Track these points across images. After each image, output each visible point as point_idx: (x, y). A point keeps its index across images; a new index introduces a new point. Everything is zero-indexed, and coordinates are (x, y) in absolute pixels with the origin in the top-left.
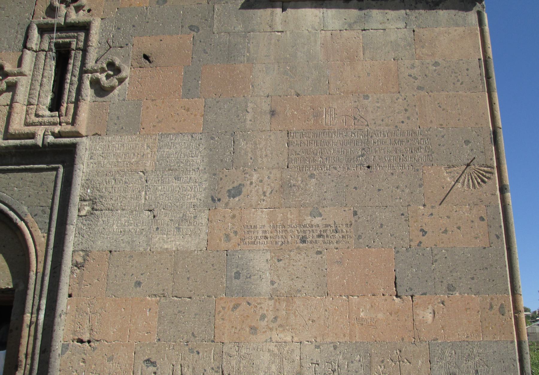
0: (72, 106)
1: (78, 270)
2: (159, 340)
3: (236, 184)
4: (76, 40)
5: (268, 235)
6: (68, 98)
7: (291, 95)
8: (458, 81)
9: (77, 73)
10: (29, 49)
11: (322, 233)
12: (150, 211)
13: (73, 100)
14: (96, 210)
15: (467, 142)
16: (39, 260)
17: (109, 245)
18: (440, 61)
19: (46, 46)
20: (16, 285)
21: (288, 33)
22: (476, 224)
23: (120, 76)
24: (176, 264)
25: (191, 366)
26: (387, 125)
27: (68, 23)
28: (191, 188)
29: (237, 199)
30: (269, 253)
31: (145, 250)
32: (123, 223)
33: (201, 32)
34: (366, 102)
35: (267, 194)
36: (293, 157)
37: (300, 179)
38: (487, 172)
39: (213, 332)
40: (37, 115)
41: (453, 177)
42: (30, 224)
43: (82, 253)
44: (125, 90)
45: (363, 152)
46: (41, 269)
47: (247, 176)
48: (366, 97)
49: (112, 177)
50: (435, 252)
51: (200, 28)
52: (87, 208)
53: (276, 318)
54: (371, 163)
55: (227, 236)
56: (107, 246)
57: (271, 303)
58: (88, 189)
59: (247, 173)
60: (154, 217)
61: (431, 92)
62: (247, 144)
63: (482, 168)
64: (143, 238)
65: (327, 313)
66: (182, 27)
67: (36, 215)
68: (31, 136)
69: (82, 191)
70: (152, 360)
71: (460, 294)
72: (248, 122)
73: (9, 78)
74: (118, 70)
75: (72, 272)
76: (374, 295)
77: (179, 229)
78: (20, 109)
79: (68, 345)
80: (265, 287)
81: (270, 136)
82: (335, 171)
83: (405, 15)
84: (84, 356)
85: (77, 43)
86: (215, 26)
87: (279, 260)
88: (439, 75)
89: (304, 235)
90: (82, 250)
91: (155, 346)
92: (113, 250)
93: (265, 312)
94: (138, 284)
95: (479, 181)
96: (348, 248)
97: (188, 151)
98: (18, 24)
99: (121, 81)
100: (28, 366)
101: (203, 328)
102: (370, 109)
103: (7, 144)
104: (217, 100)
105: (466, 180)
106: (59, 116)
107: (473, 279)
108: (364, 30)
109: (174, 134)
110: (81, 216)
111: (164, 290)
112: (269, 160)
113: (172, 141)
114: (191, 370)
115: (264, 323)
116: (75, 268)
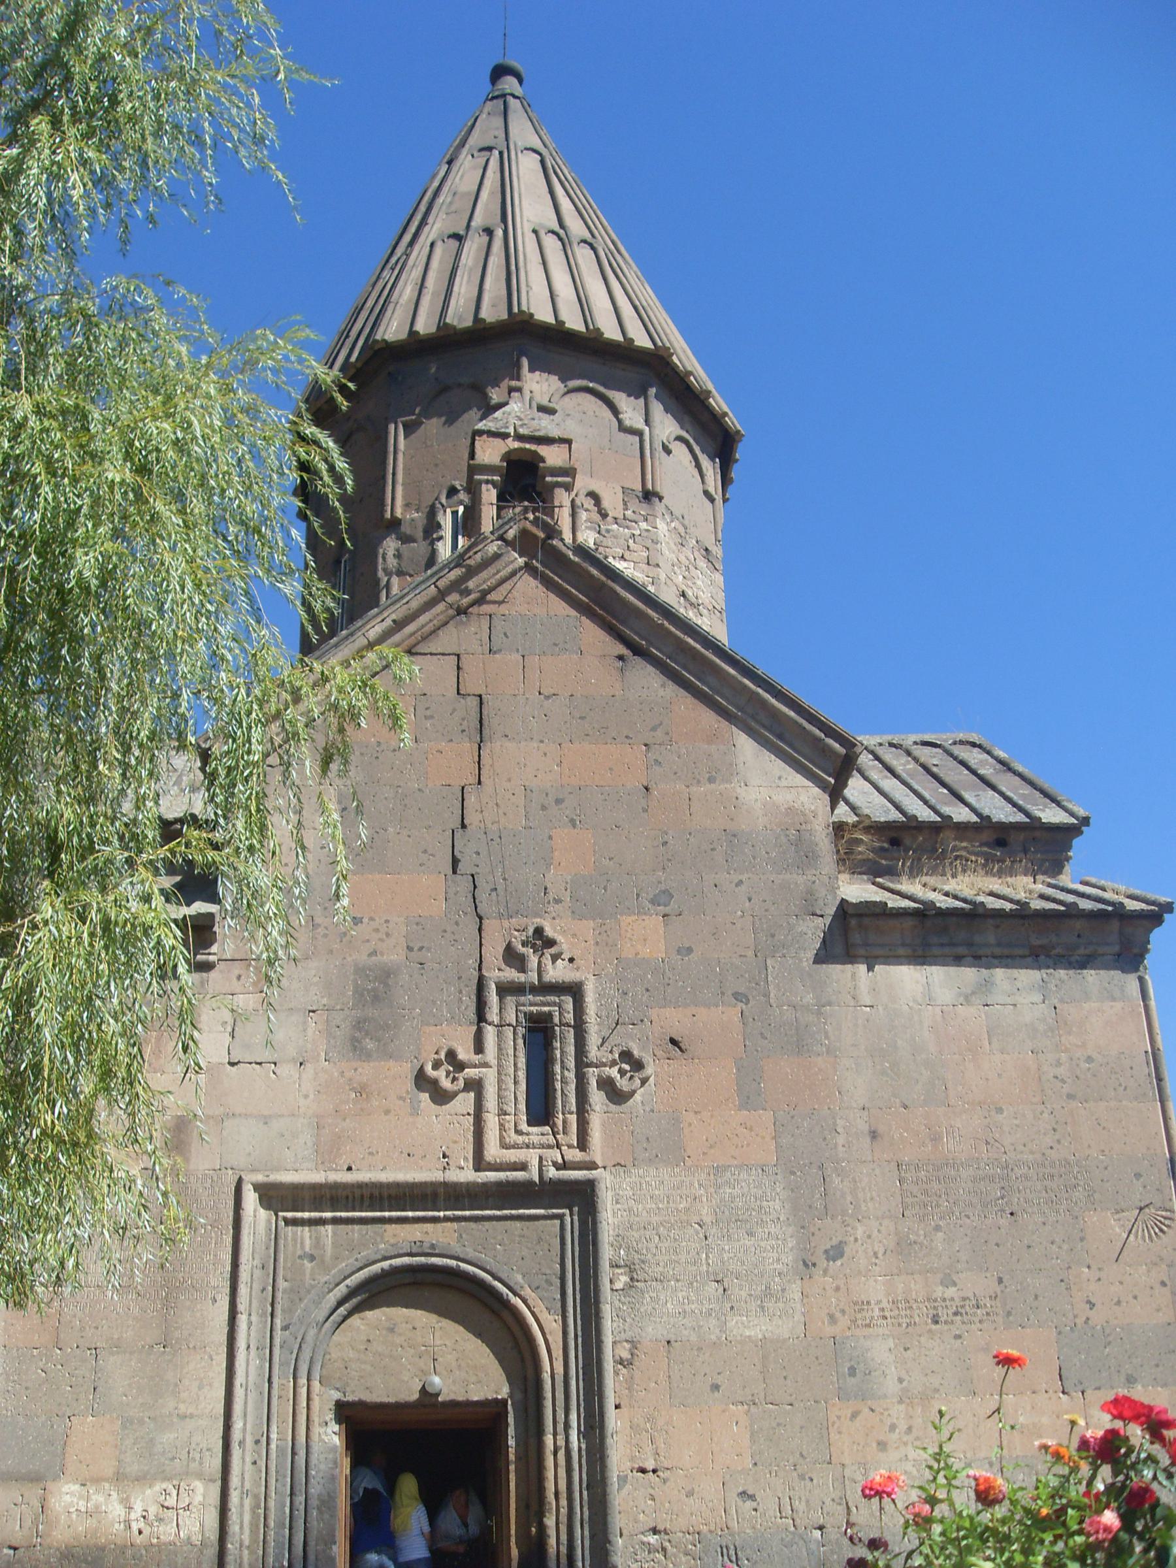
0: (573, 1119)
1: (624, 1370)
2: (756, 1464)
3: (835, 1242)
4: (557, 1008)
5: (887, 1314)
6: (564, 1106)
7: (895, 1107)
8: (1120, 1085)
9: (571, 1063)
10: (490, 1024)
11: (960, 1309)
12: (718, 1282)
13: (574, 1109)
14: (638, 1281)
15: (1138, 1176)
16: (554, 1355)
17: (665, 1333)
18: (1095, 1055)
19: (511, 1017)
21: (880, 1008)
22: (1157, 1291)
23: (643, 1074)
24: (765, 1357)
25: (803, 1498)
26: (1032, 1152)
27: (546, 983)
28: (773, 1248)
29: (839, 1263)
30: (891, 1340)
31: (719, 1338)
32: (681, 1299)
33: (752, 1003)
34: (1000, 1117)
35: (880, 1255)
36: (909, 1200)
37: (922, 1232)
38: (1165, 1218)
39: (828, 1451)
40: (518, 1132)
41: (1123, 1226)
42: (530, 1302)
43: (627, 1346)
45: (1003, 1191)
46: (559, 1369)
47: (849, 1229)
48: (1000, 1110)
49: (654, 1232)
50: (1107, 1332)
51: (750, 998)
53: (910, 1429)
54: (1015, 1209)
55: (831, 1317)
57: (902, 1407)
58: (620, 1249)
59: (848, 1225)
60: (724, 1290)
61: (1086, 1101)
62: (842, 1181)
63: (1159, 1213)
64: (713, 1322)
65: (976, 1419)
66: (723, 993)
68: (520, 1166)
69: (611, 1253)
70: (749, 1493)
71: (1143, 1386)
72: (840, 1149)
73: (467, 1070)
74: (638, 1065)
75: (616, 1373)
76: (1034, 1392)
77: (763, 1308)
78: (491, 1121)
80: (891, 1386)
81: (873, 1170)
82: (968, 1221)
83: (1041, 983)
84: (652, 1492)
85: (560, 1012)
86: (772, 995)
87: (906, 1349)
88: (1095, 1076)
89: (935, 1312)
90: (627, 1341)
91: (751, 1473)
92: (672, 1340)
93: (895, 1421)
94: (716, 1387)
95: (1157, 1230)
96: (995, 1329)
97: (760, 1192)
99: (644, 1081)
101: (814, 1445)
102: (1006, 1129)
103: (485, 1180)
104: (791, 1114)
105: (1140, 1230)
107: (1157, 1366)
108: (987, 1005)
110: (617, 1290)
111: (753, 1395)
112: (877, 1205)
113: (735, 1177)
114: (803, 1503)
115: (895, 1436)
116: (620, 1367)
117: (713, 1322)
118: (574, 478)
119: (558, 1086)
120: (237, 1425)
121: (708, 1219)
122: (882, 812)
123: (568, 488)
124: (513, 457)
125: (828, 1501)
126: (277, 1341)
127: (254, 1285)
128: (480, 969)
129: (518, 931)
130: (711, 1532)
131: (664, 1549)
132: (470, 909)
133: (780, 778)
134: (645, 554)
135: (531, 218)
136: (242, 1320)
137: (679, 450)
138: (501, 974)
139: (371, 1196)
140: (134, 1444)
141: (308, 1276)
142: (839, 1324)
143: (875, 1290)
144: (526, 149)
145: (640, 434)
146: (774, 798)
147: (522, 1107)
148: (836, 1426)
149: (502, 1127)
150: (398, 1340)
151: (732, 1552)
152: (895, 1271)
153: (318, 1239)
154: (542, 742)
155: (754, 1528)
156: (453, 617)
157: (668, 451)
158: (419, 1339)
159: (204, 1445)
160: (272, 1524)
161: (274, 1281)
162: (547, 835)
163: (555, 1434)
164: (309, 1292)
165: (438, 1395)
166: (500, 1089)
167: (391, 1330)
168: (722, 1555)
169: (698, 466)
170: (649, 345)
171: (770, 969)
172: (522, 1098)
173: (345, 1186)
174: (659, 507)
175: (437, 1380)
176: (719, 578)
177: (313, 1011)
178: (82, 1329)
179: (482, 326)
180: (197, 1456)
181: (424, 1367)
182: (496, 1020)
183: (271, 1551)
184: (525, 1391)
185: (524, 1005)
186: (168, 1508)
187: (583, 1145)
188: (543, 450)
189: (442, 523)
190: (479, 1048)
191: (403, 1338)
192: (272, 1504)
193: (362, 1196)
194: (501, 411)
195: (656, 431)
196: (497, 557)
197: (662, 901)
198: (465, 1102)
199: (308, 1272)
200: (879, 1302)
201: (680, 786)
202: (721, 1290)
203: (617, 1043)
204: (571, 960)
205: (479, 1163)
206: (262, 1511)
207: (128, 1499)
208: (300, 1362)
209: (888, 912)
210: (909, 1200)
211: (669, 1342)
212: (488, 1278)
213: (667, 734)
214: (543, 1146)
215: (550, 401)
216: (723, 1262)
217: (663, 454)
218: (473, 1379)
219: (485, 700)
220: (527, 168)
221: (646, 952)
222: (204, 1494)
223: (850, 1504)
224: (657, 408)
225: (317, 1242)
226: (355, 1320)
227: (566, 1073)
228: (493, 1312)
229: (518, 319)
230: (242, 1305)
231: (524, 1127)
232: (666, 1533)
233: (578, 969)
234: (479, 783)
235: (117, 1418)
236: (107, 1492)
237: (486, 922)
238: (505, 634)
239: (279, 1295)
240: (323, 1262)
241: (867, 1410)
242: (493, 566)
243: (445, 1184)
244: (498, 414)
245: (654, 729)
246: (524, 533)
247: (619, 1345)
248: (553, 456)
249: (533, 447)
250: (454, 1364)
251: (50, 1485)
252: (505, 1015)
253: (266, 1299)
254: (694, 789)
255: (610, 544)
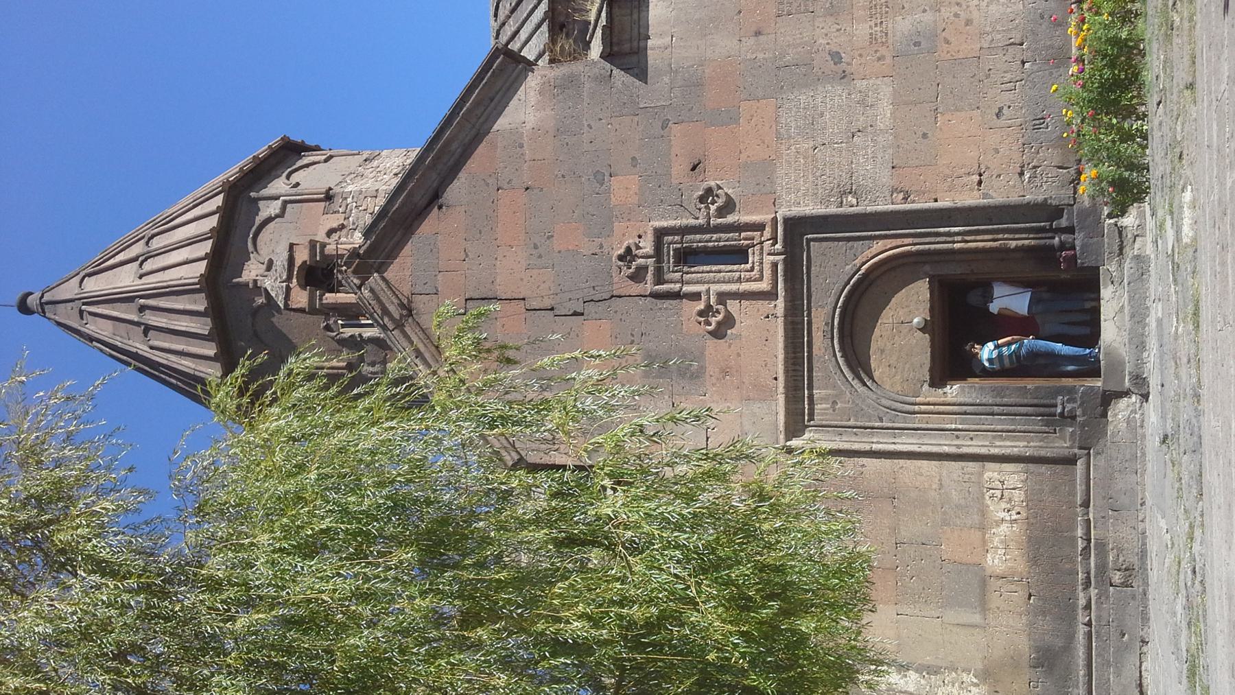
0: (743, 235)
3: (829, 58)
5: (879, 21)
6: (736, 240)
20: (926, 275)
24: (906, 104)
28: (831, 100)
29: (843, 55)
30: (896, 18)
35: (839, 27)
36: (803, 8)
40: (752, 269)
42: (864, 260)
43: (895, 195)
44: (728, 183)
47: (820, 49)
52: (850, 198)
53: (958, 4)
55: (879, 59)
56: (887, 172)
60: (859, 131)
64: (880, 139)
66: (662, 136)
67: (855, 255)
68: (774, 268)
72: (766, 56)
74: (709, 191)
75: (913, 202)
78: (745, 287)
79: (983, 194)
80: (928, 17)
84: (994, 176)
87: (903, 8)
90: (892, 195)
94: (925, 136)
98: (651, 309)
99: (719, 188)
100: (1005, 236)
106: (754, 246)
109: (777, 126)
114: (1006, 75)
115: (962, 13)
117: (880, 139)
118: (317, 242)
119: (722, 244)
120: (946, 449)
121: (811, 144)
122: (544, 34)
123: (323, 245)
124: (303, 282)
125: (1005, 58)
126: (890, 425)
127: (853, 440)
128: (645, 296)
129: (621, 272)
130: (1023, 137)
131: (1035, 167)
132: (607, 303)
133: (520, 100)
134: (370, 199)
135: (131, 280)
136: (875, 447)
137: (295, 178)
138: (649, 282)
139: (794, 364)
140: (959, 518)
141: (846, 405)
142: (884, 54)
143: (862, 30)
144: (80, 287)
145: (285, 203)
146: (533, 103)
147: (735, 267)
148: (954, 54)
149: (748, 280)
150: (889, 345)
151: (1037, 122)
152: (849, 17)
153: (822, 399)
154: (496, 259)
155: (1021, 108)
156: (414, 319)
157: (297, 184)
158: (889, 332)
159: (960, 472)
160: (1013, 427)
161: (849, 427)
162: (558, 254)
163: (954, 242)
164: (857, 405)
165: (926, 320)
166: (724, 282)
167: (882, 351)
168: (1040, 128)
169: (307, 166)
170: (221, 196)
171: (646, 105)
172: (730, 267)
173: (786, 381)
174: (337, 190)
175: (916, 320)
176: (385, 153)
177: (673, 404)
178: (883, 553)
179: (210, 310)
180: (967, 476)
181: (908, 329)
182: (678, 286)
183: (1030, 428)
184: (925, 263)
185: (669, 268)
186: (1002, 495)
187: (760, 227)
188: (298, 262)
189: (350, 334)
190: (696, 296)
191: (888, 344)
192: (999, 427)
193: (794, 370)
194: (271, 293)
195: (283, 192)
196: (372, 290)
197: (601, 178)
198: (733, 305)
199: (844, 405)
200: (871, 27)
201: (525, 167)
202: (859, 134)
203: (694, 206)
204: (640, 237)
205: (771, 295)
206: (1004, 434)
207: (996, 522)
208: (904, 409)
209: (609, 25)
210: (803, 8)
211: (893, 167)
212: (848, 287)
213: (490, 176)
214: (761, 253)
215: (263, 264)
216: (840, 133)
217: (299, 188)
218: (916, 297)
219: (469, 297)
220: (94, 286)
221: (634, 188)
222: (992, 472)
223: (1008, 43)
224: (265, 192)
225: (824, 399)
226: (876, 375)
227: (713, 239)
228: (870, 285)
229: (205, 285)
230: (867, 447)
231: (749, 266)
232: (1023, 166)
233: (645, 233)
234: (524, 299)
235: (942, 529)
236: (992, 535)
237: (615, 293)
238: (425, 284)
239: (859, 424)
240: (836, 396)
241: (944, 33)
242: (378, 293)
243: (785, 316)
244: (273, 295)
245: (488, 185)
246: (354, 272)
247: (894, 201)
248: (302, 256)
249: (296, 269)
250: (906, 310)
251: (988, 572)
252: (675, 279)
253: (862, 432)
254: (527, 158)
255: (363, 222)
